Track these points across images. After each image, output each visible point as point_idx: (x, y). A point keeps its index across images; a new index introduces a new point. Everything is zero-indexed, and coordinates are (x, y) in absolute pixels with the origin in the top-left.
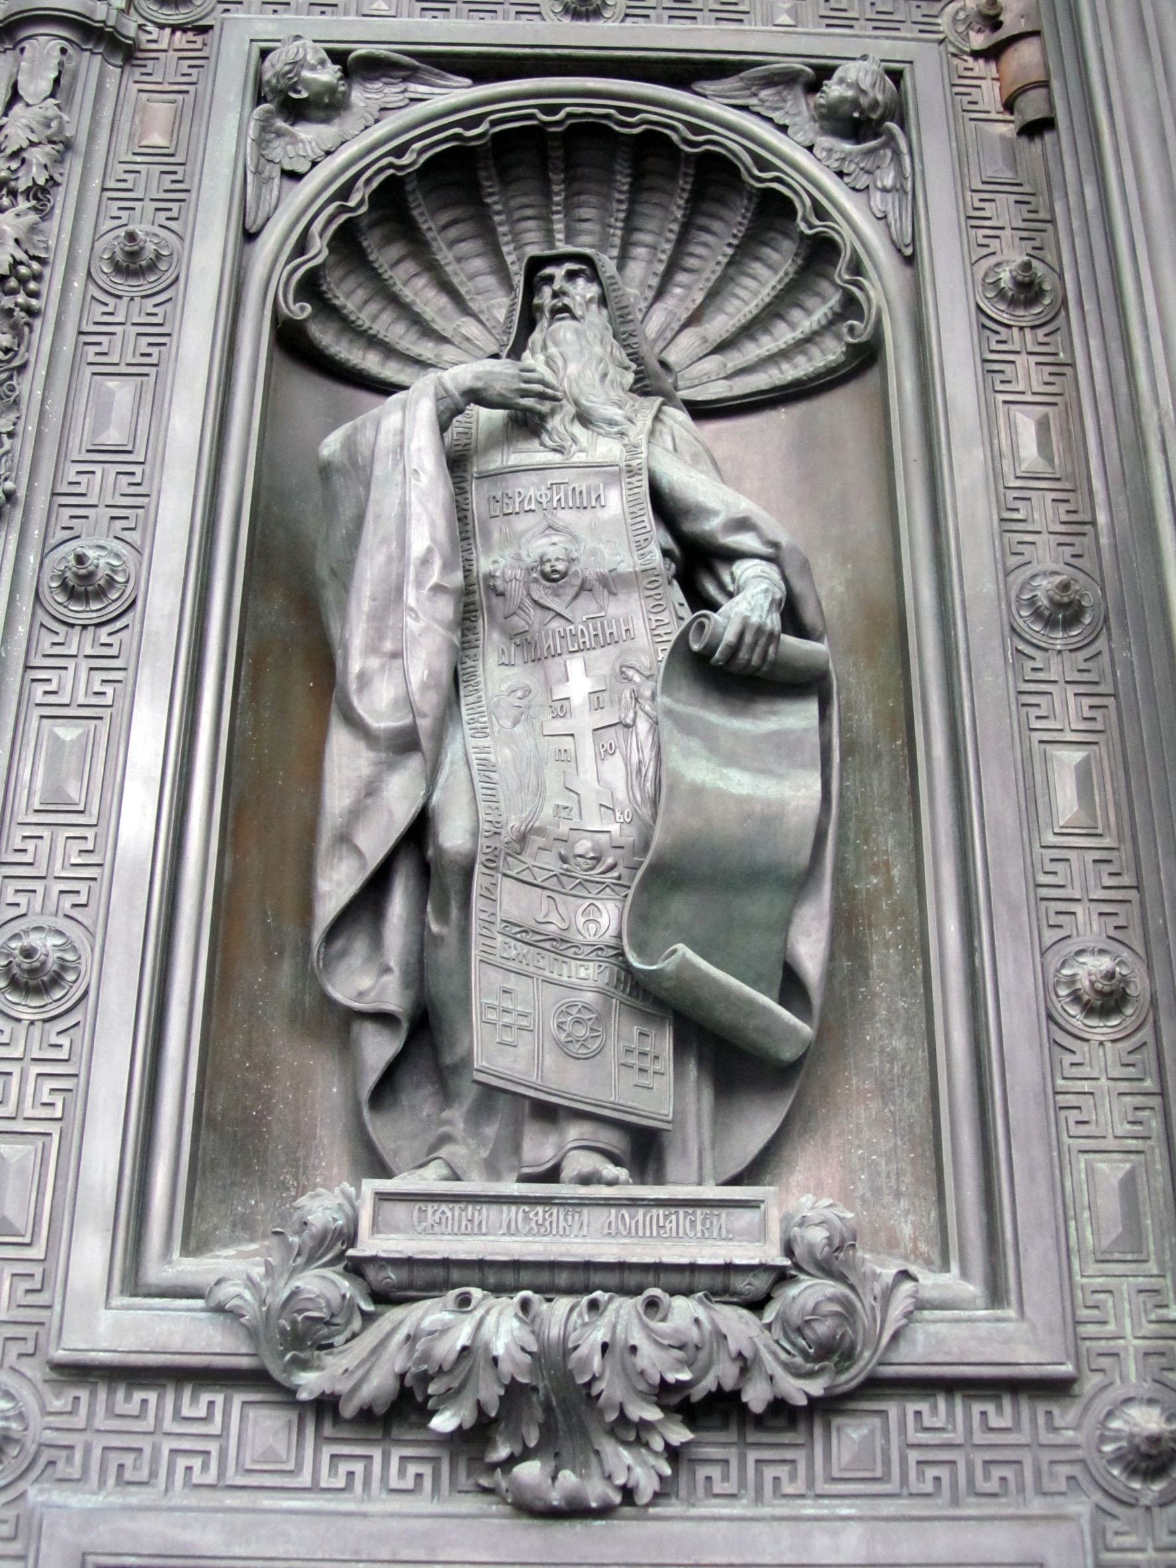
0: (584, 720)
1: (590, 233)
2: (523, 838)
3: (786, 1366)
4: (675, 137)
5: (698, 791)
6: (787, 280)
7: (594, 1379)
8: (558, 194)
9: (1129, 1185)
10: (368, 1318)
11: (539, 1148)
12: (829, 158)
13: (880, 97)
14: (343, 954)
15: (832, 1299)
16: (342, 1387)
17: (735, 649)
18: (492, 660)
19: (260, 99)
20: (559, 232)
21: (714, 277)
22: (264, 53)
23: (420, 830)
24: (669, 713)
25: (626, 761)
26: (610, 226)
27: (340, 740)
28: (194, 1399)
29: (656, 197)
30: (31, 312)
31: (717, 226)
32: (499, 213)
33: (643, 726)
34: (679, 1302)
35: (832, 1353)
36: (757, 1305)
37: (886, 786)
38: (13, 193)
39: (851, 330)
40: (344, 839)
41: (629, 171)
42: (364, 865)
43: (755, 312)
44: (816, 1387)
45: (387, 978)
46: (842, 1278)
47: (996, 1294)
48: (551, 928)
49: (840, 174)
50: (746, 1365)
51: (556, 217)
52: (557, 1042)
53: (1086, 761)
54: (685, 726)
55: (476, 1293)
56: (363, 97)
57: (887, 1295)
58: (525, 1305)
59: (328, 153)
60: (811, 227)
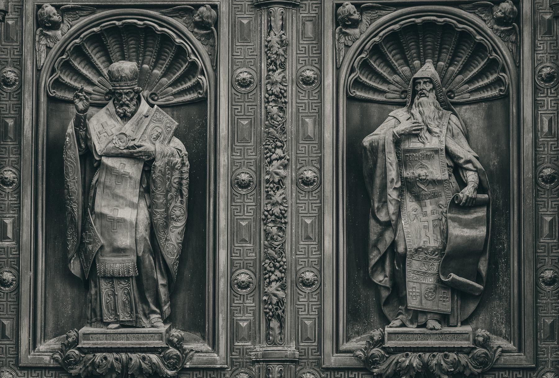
0: (431, 218)
2: (416, 250)
3: (473, 366)
5: (457, 236)
7: (434, 371)
9: (552, 325)
10: (387, 358)
11: (422, 319)
12: (497, 32)
14: (376, 270)
15: (483, 353)
16: (383, 372)
17: (464, 204)
18: (408, 200)
22: (338, 5)
23: (394, 244)
24: (450, 218)
25: (440, 228)
27: (372, 222)
28: (352, 374)
30: (285, 103)
31: (467, 45)
33: (444, 219)
34: (451, 354)
35: (483, 364)
36: (468, 354)
37: (504, 222)
38: (276, 64)
40: (375, 246)
42: (380, 253)
44: (479, 371)
45: (386, 279)
46: (486, 348)
47: (520, 350)
48: (423, 270)
50: (466, 367)
52: (425, 297)
53: (552, 220)
54: (454, 220)
55: (410, 353)
56: (366, 18)
57: (495, 352)
58: (420, 356)
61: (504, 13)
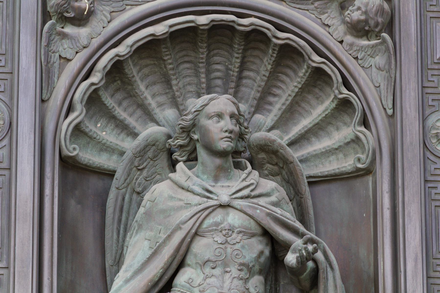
1: (218, 70)
4: (269, 34)
6: (327, 112)
8: (203, 54)
13: (380, 20)
19: (46, 16)
20: (202, 73)
21: (288, 103)
26: (231, 70)
29: (256, 53)
32: (170, 64)
39: (359, 160)
41: (243, 43)
43: (310, 126)
49: (356, 58)
51: (201, 65)
59: (84, 47)
60: (341, 93)
61: (366, 13)
